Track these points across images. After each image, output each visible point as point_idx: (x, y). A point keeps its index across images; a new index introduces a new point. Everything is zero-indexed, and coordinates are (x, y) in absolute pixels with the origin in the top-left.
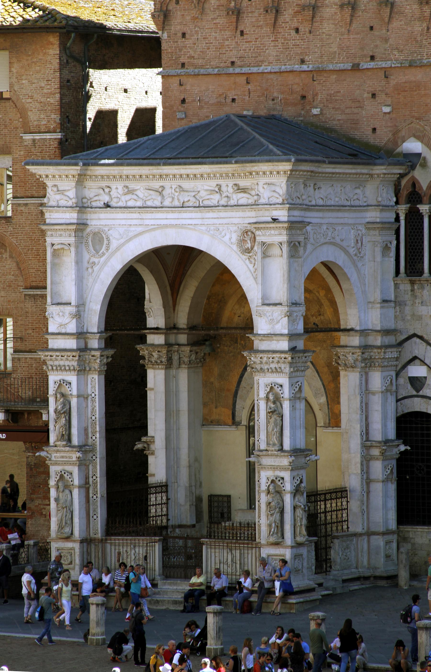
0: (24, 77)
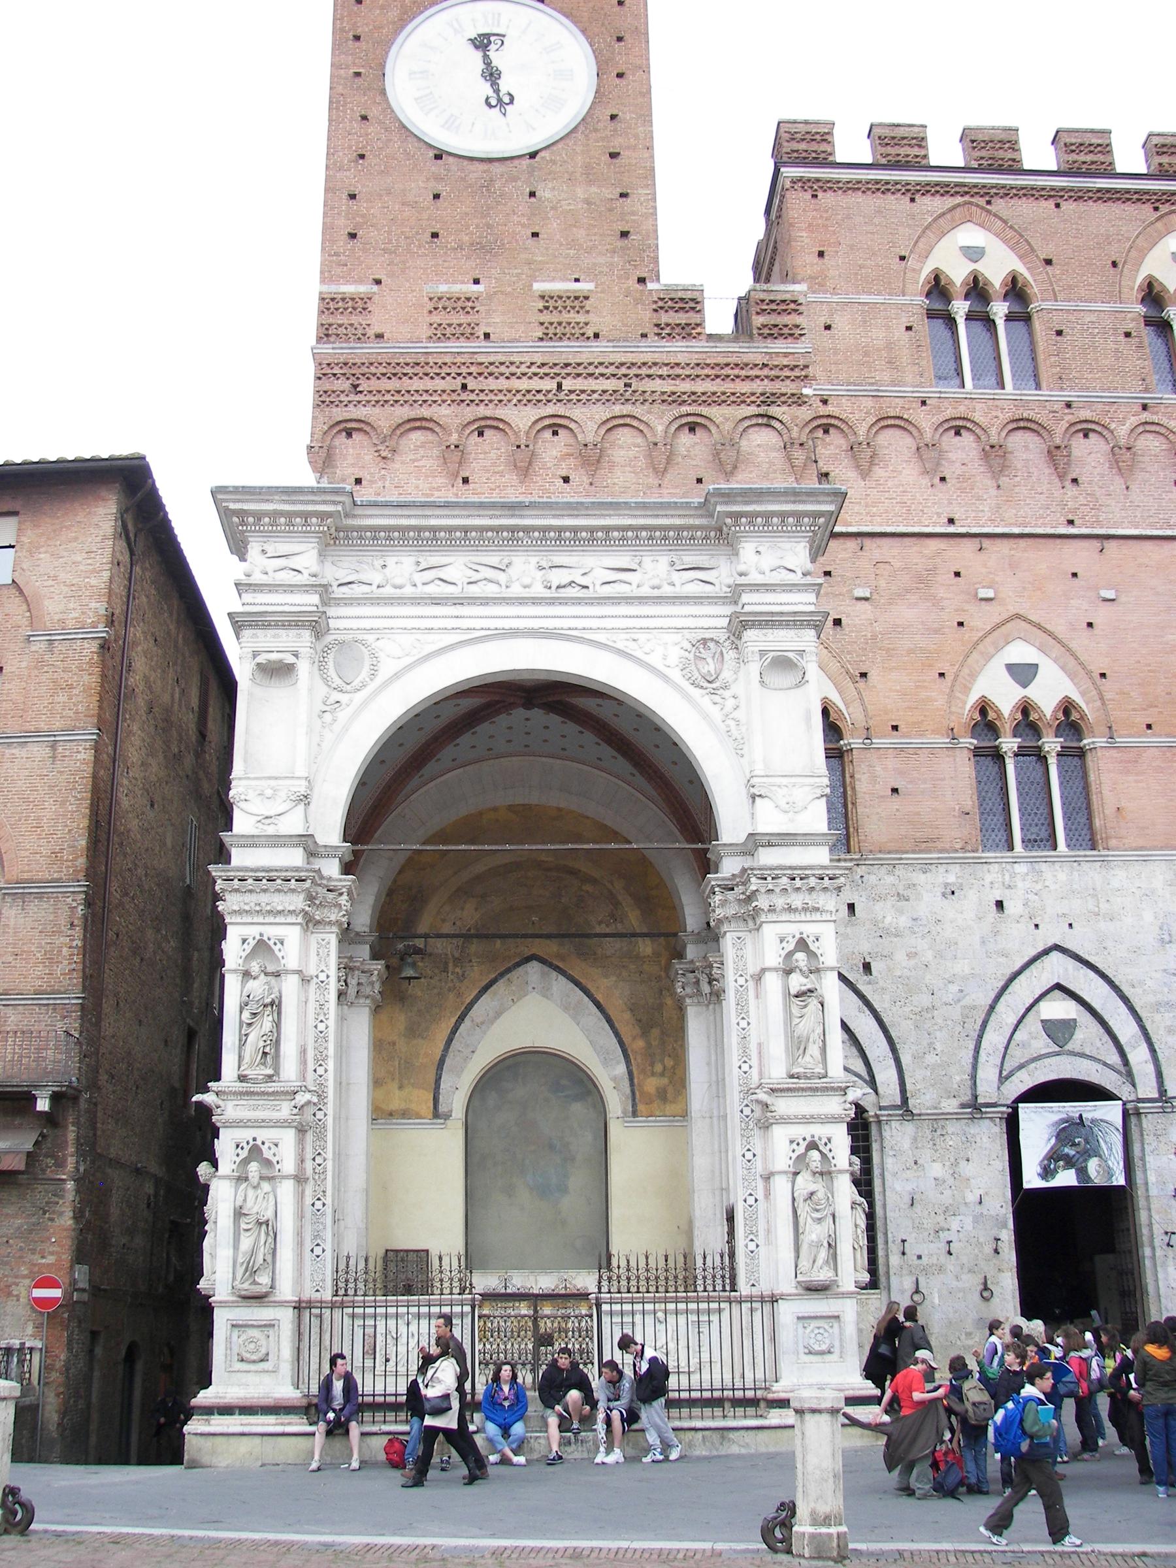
0: (42, 550)
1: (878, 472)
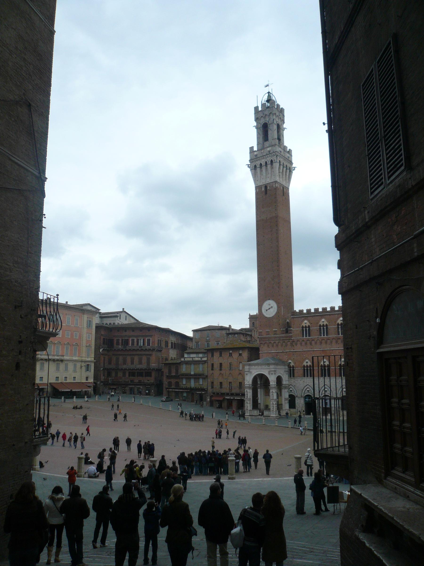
1: (297, 345)
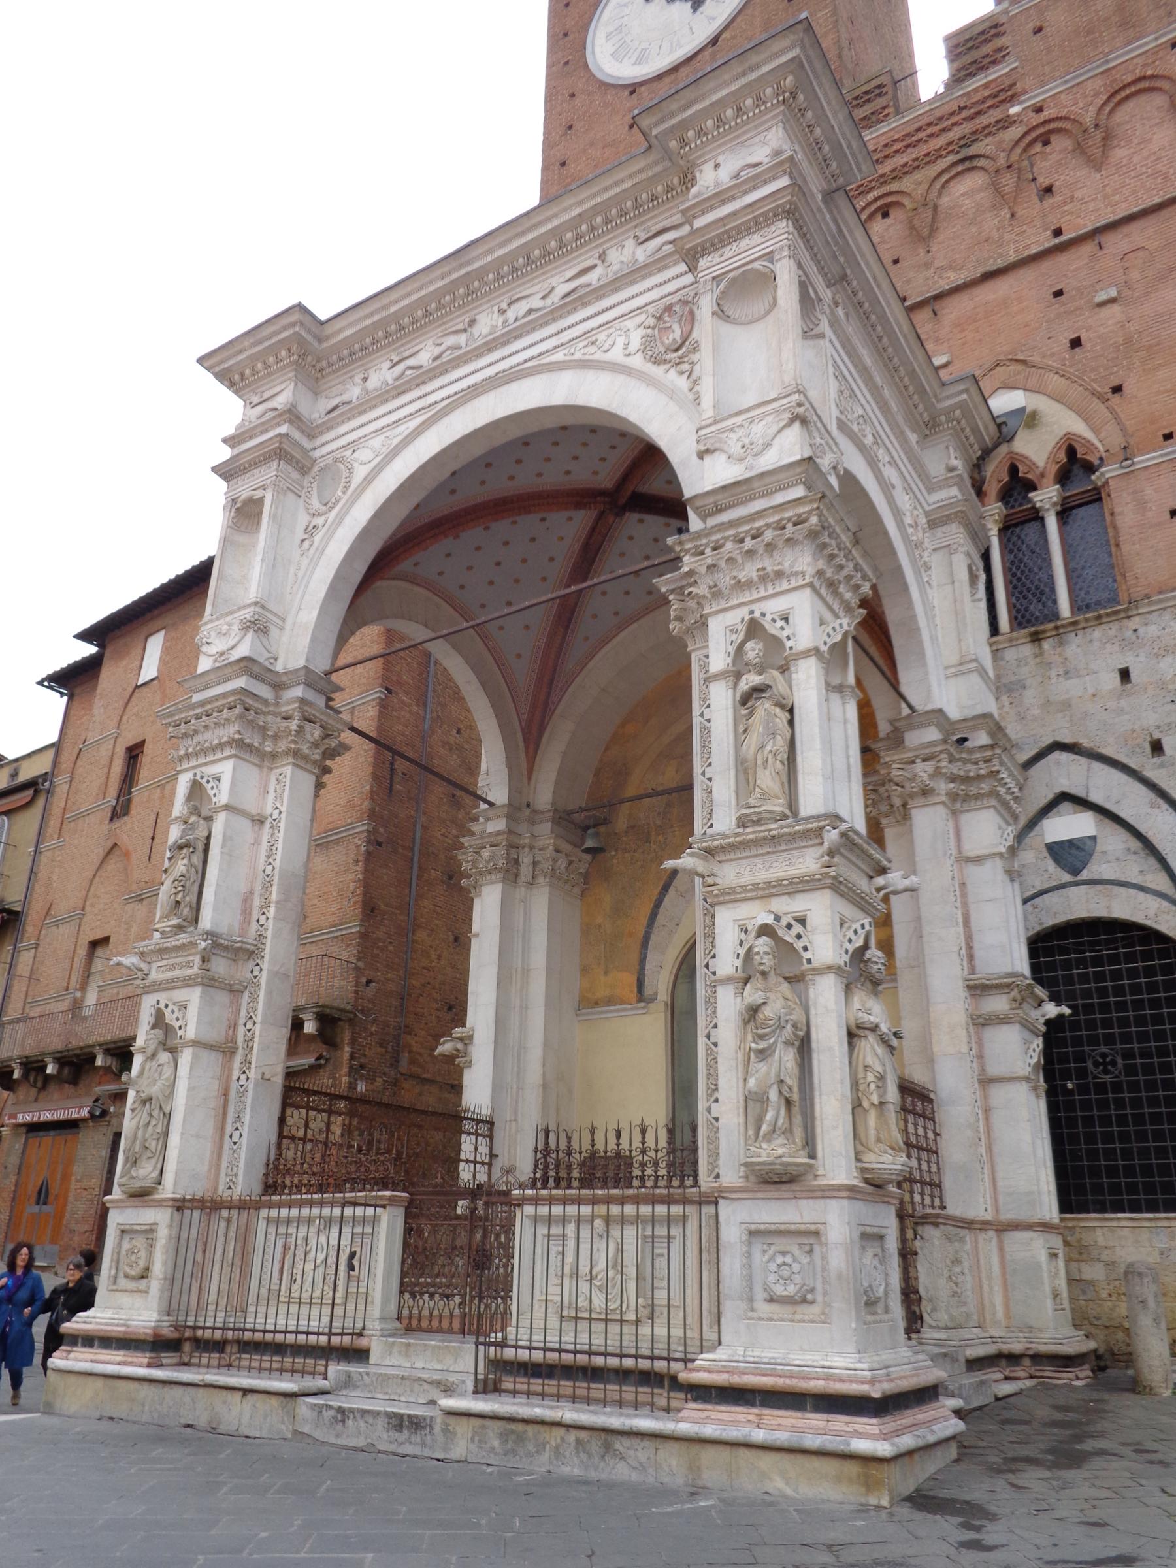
1: (1119, 153)
